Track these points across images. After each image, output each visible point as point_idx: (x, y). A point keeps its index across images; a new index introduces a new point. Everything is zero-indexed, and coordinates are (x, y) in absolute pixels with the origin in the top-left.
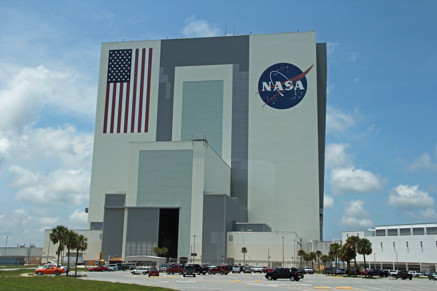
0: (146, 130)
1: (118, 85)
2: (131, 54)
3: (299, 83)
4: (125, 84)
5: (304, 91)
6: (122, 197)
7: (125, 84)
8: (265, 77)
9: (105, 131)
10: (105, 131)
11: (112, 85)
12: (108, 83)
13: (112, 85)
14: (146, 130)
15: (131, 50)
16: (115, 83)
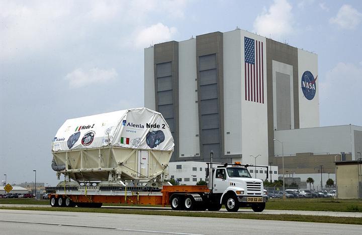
0: (263, 103)
1: (250, 64)
2: (254, 43)
3: (313, 85)
4: (253, 65)
5: (315, 90)
6: (351, 154)
7: (253, 65)
8: (303, 79)
9: (246, 100)
10: (246, 100)
11: (247, 63)
12: (246, 62)
13: (247, 63)
14: (263, 103)
15: (254, 40)
16: (249, 63)
